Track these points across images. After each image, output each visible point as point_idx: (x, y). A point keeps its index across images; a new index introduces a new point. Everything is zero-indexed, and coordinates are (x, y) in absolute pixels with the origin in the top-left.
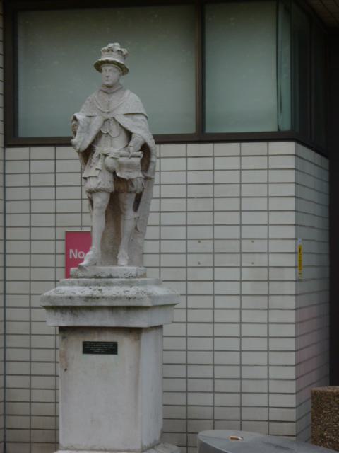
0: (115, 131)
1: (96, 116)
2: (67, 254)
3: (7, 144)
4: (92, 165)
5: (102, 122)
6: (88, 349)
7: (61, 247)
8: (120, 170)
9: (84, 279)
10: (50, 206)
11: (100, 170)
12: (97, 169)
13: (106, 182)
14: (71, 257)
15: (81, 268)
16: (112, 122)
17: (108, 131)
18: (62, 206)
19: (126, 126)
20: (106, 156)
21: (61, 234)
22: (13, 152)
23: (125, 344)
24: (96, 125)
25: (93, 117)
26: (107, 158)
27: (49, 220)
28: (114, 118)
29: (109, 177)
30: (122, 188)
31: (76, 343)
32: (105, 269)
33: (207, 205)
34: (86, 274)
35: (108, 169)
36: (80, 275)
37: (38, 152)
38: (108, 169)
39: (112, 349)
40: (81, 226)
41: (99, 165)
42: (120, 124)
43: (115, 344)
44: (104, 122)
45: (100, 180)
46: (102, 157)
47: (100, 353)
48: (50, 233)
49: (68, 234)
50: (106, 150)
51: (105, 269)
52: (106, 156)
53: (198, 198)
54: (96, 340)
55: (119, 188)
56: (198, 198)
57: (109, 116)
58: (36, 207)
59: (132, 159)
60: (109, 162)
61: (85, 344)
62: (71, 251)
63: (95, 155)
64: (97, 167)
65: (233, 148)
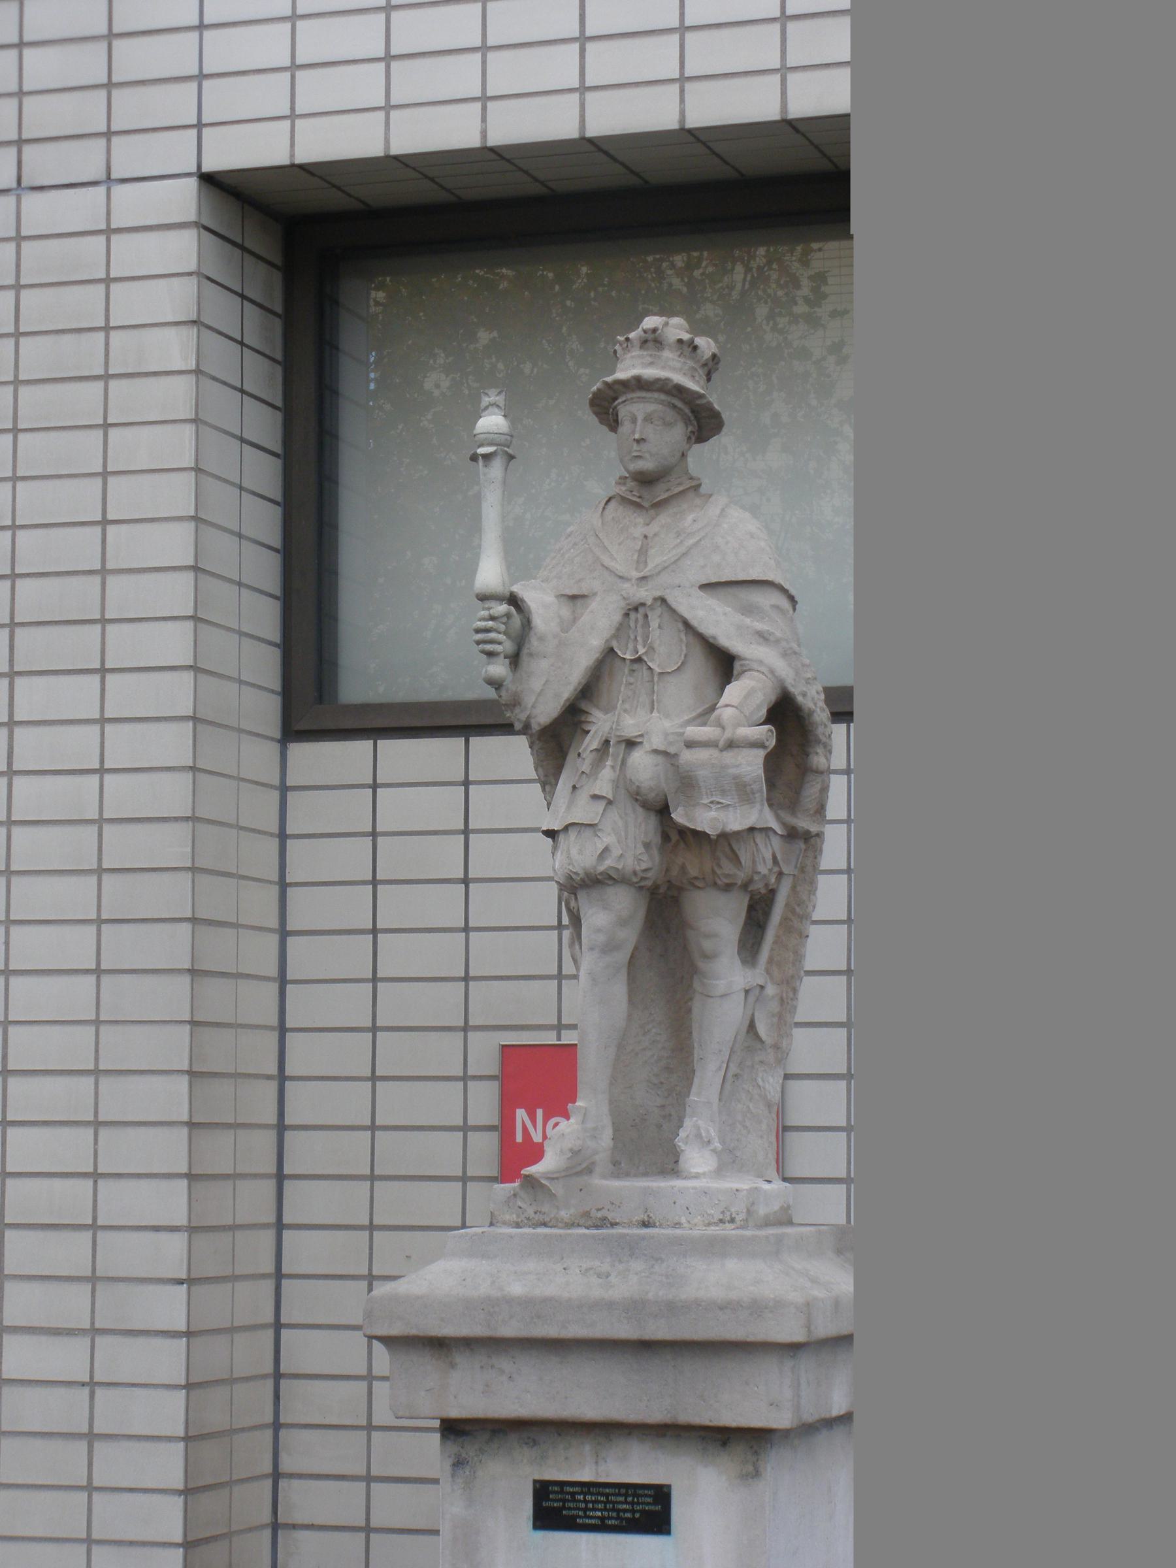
0: (665, 648)
1: (595, 594)
2: (506, 1126)
3: (294, 730)
5: (617, 617)
6: (556, 1509)
7: (485, 1103)
10: (443, 954)
11: (610, 802)
12: (595, 797)
14: (519, 1138)
17: (641, 651)
18: (489, 954)
19: (708, 630)
20: (631, 744)
21: (484, 1053)
22: (315, 759)
23: (704, 1494)
24: (597, 626)
25: (583, 596)
27: (444, 1003)
28: (663, 600)
29: (644, 827)
30: (693, 872)
31: (511, 1480)
35: (638, 798)
37: (401, 755)
38: (638, 798)
39: (648, 1512)
40: (559, 1027)
41: (604, 783)
42: (687, 624)
43: (661, 1495)
44: (627, 615)
45: (607, 839)
47: (602, 1527)
48: (444, 1054)
49: (507, 1051)
50: (630, 725)
52: (631, 744)
54: (586, 1475)
57: (645, 594)
58: (397, 955)
60: (643, 767)
61: (542, 1490)
62: (521, 1114)
63: (591, 742)
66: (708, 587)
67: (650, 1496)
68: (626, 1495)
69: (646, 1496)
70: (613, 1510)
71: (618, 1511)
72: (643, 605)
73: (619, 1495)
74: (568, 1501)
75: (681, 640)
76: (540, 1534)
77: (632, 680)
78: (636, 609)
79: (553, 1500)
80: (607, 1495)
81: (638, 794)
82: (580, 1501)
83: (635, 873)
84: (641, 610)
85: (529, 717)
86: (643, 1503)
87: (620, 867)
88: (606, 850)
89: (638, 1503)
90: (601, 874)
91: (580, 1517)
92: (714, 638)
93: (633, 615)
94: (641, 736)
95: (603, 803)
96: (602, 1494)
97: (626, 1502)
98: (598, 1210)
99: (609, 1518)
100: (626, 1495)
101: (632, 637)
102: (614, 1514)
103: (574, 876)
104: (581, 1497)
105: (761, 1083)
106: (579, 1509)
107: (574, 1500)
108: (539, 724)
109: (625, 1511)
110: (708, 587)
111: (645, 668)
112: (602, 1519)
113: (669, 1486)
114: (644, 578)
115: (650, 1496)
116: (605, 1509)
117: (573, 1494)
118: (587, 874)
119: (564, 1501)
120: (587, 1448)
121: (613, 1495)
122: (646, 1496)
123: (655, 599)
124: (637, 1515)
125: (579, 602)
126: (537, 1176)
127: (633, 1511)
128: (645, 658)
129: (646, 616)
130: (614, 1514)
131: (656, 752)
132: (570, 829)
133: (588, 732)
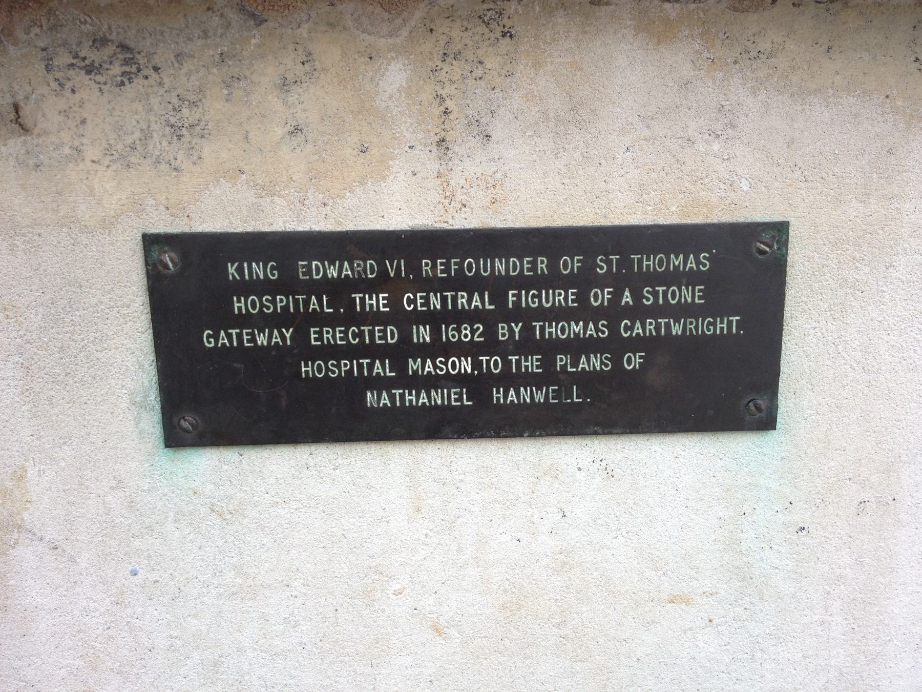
6: (266, 351)
39: (671, 340)
54: (398, 202)
67: (692, 278)
68: (584, 282)
69: (672, 278)
70: (527, 345)
71: (549, 349)
73: (553, 281)
74: (320, 320)
76: (208, 465)
79: (243, 321)
80: (497, 287)
82: (376, 318)
86: (656, 311)
89: (638, 312)
91: (380, 384)
96: (473, 285)
97: (583, 312)
99: (509, 379)
100: (584, 282)
102: (532, 364)
104: (379, 302)
106: (374, 352)
107: (353, 318)
109: (578, 347)
112: (478, 385)
113: (779, 231)
115: (692, 278)
116: (491, 345)
117: (339, 290)
119: (302, 321)
120: (395, 76)
121: (522, 283)
122: (672, 278)
124: (633, 361)
127: (615, 346)
130: (532, 364)
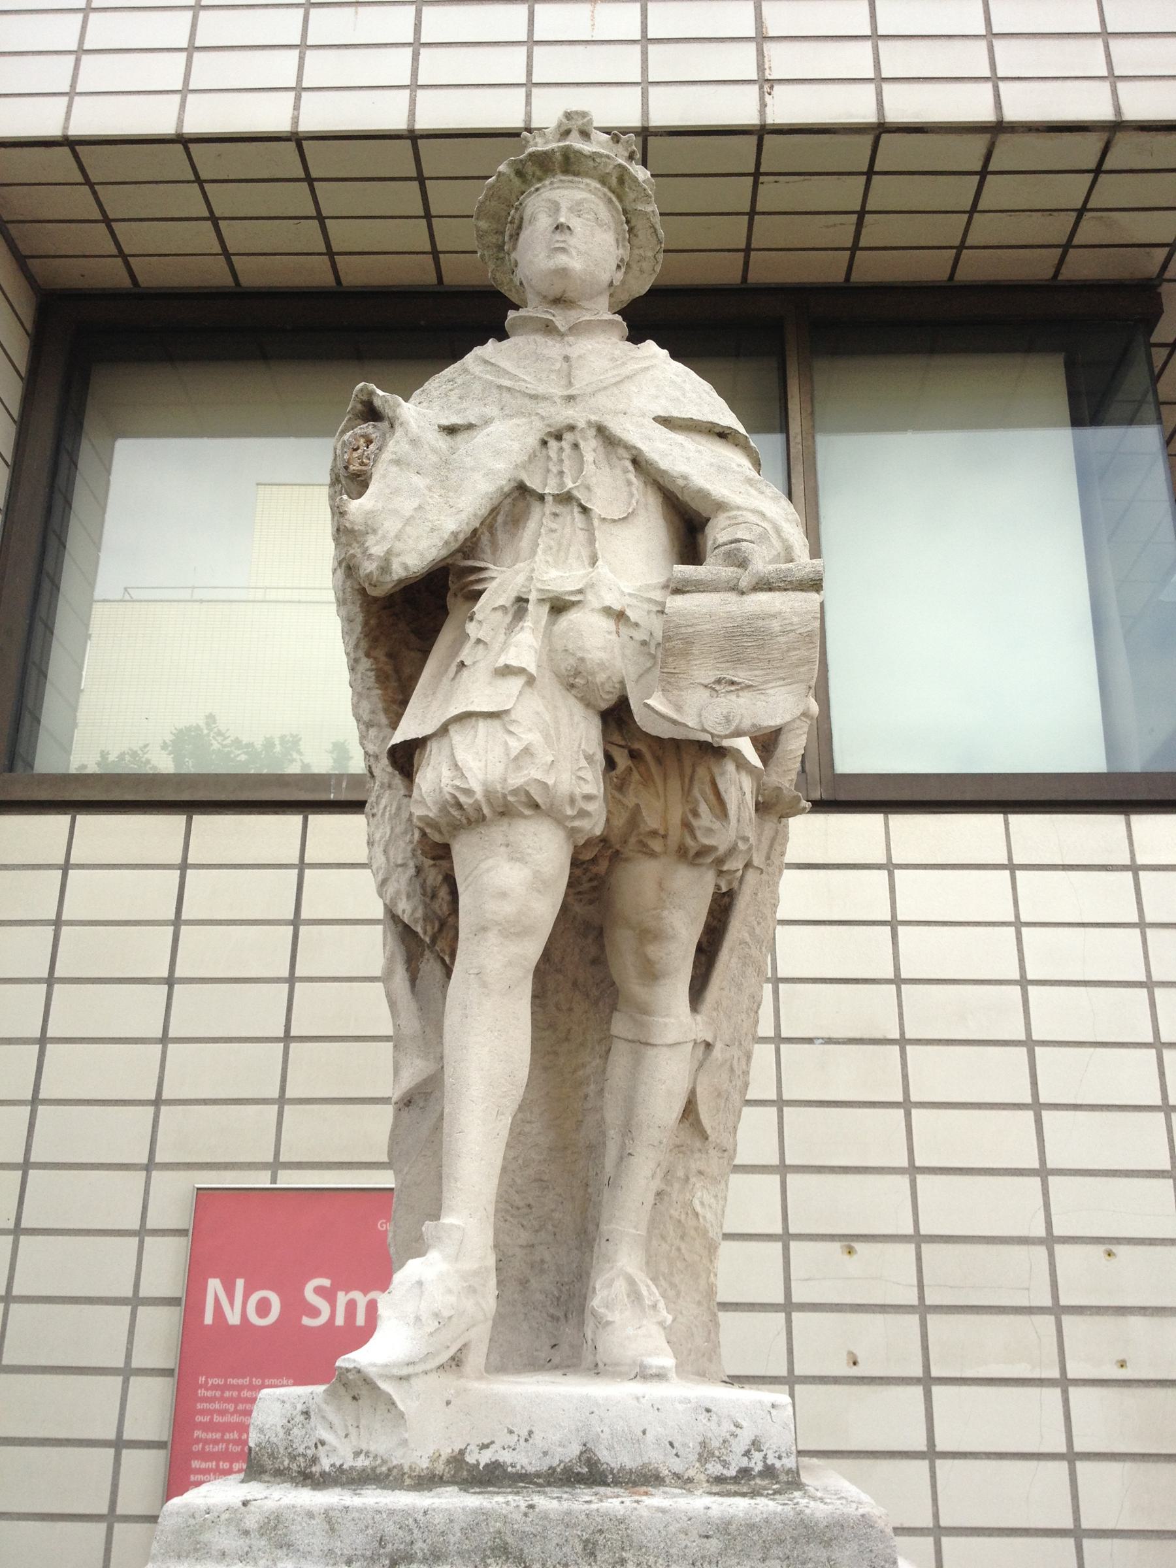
0: (608, 488)
4: (465, 655)
5: (532, 441)
8: (670, 682)
9: (372, 1498)
11: (531, 681)
12: (507, 671)
13: (561, 754)
15: (359, 1390)
16: (590, 447)
20: (558, 607)
25: (470, 427)
26: (572, 617)
28: (601, 431)
29: (585, 734)
32: (549, 1407)
33: (876, 1074)
34: (382, 1444)
35: (574, 680)
36: (339, 1452)
38: (574, 680)
42: (638, 462)
44: (544, 443)
45: (527, 734)
46: (537, 613)
51: (549, 1407)
52: (558, 607)
53: (829, 1041)
55: (635, 817)
56: (829, 1041)
57: (577, 415)
59: (763, 599)
64: (511, 658)
65: (977, 833)
66: (666, 422)
72: (572, 428)
75: (629, 483)
77: (554, 526)
78: (559, 437)
81: (577, 673)
83: (572, 801)
84: (568, 437)
85: (389, 552)
87: (550, 782)
88: (527, 751)
90: (515, 792)
92: (685, 478)
93: (553, 444)
94: (580, 591)
95: (519, 682)
98: (485, 1447)
101: (554, 470)
103: (463, 799)
105: (699, 1209)
108: (406, 568)
110: (666, 422)
111: (576, 510)
114: (570, 398)
118: (489, 794)
123: (590, 424)
125: (460, 438)
126: (372, 1372)
128: (576, 493)
129: (576, 446)
131: (608, 611)
132: (453, 730)
133: (480, 593)
